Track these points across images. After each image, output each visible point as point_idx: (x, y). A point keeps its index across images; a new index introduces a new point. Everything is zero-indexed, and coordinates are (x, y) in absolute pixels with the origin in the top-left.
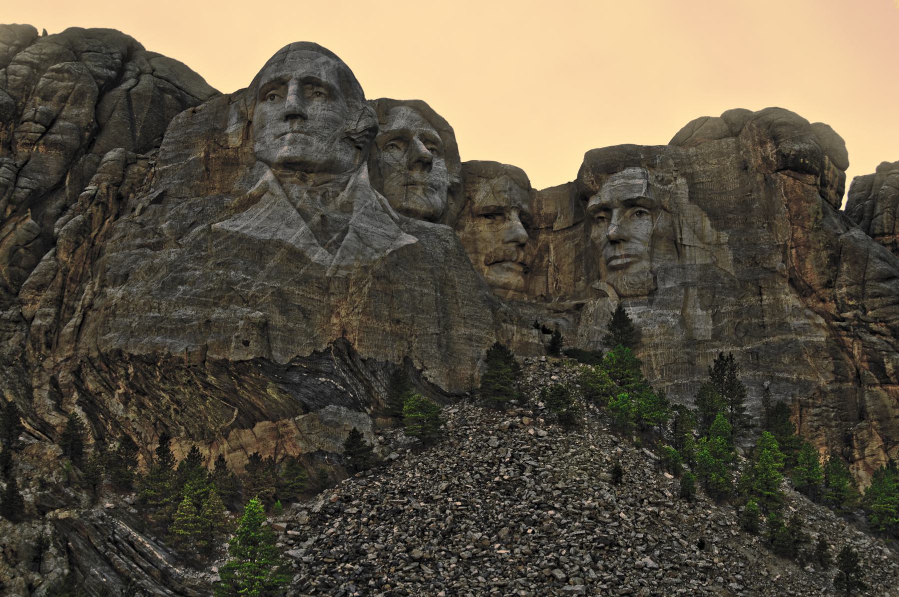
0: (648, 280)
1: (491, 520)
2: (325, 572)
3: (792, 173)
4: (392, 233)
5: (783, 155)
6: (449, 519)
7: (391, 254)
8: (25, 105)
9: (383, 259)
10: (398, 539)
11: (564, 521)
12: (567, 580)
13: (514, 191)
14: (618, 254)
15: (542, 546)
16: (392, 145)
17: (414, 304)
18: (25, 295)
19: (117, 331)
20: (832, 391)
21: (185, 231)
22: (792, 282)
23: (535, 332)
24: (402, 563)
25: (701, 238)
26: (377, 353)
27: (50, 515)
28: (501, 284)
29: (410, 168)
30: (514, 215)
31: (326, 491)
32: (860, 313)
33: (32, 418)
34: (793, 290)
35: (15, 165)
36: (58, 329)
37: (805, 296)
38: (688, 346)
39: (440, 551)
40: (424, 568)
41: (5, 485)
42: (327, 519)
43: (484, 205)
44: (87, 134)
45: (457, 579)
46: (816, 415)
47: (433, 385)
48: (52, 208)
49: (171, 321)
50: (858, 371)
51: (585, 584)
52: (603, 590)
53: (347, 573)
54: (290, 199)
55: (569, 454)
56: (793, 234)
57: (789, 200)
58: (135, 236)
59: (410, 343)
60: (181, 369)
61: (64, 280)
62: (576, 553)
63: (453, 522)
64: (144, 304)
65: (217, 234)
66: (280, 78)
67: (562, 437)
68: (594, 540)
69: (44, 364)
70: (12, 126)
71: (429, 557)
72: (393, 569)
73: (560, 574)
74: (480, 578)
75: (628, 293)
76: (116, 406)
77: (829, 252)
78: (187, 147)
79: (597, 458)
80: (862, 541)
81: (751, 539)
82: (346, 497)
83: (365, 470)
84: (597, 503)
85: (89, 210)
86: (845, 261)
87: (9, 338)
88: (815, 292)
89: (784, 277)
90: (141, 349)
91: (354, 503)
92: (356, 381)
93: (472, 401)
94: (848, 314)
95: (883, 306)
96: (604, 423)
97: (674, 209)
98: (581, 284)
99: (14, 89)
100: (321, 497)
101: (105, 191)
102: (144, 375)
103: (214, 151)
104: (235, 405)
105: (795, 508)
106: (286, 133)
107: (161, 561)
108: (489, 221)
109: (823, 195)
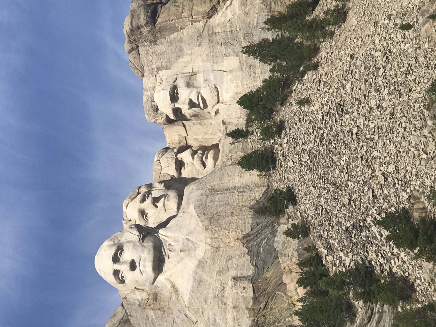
0: (211, 89)
1: (329, 165)
4: (189, 216)
5: (147, 23)
6: (330, 186)
9: (202, 221)
10: (339, 211)
12: (358, 126)
13: (168, 156)
15: (341, 139)
17: (223, 205)
22: (210, 18)
25: (189, 63)
28: (214, 162)
29: (156, 207)
30: (180, 156)
34: (213, 17)
38: (242, 69)
39: (345, 190)
45: (359, 182)
46: (275, 4)
47: (263, 195)
53: (357, 237)
56: (186, 18)
59: (243, 207)
60: (258, 320)
63: (330, 184)
65: (190, 303)
68: (338, 113)
71: (348, 196)
73: (355, 131)
78: (148, 319)
79: (298, 113)
81: (337, 35)
84: (320, 112)
89: (207, 21)
91: (322, 233)
93: (270, 175)
96: (281, 109)
97: (175, 77)
100: (319, 250)
103: (150, 305)
104: (275, 293)
108: (183, 168)
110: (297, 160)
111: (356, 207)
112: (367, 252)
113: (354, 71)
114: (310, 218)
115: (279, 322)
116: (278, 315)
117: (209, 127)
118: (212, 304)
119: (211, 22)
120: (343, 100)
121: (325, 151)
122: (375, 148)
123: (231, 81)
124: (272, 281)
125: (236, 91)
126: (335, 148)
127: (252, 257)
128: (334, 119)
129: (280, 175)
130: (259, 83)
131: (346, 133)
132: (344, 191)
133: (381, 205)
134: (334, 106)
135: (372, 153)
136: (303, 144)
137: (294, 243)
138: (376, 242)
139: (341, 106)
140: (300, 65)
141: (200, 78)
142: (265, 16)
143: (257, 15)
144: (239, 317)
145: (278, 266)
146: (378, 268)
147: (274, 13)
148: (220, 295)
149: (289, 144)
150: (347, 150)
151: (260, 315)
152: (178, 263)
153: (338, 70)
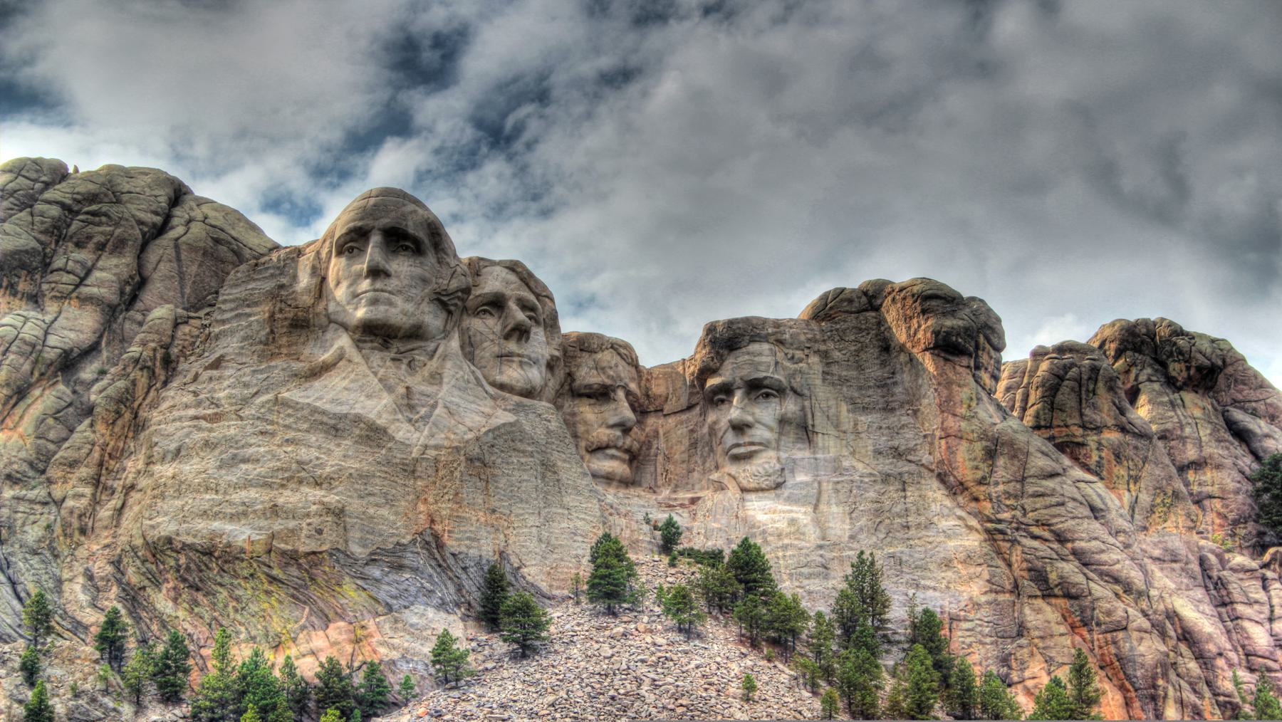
0: (774, 472)
4: (487, 410)
7: (486, 433)
8: (55, 251)
9: (477, 439)
13: (621, 368)
16: (485, 311)
18: (54, 472)
19: (166, 514)
21: (245, 401)
22: (942, 478)
23: (646, 528)
25: (837, 426)
26: (469, 547)
29: (507, 337)
30: (621, 394)
31: (410, 704)
32: (1018, 513)
34: (941, 486)
36: (93, 514)
38: (821, 547)
44: (128, 289)
48: (87, 372)
49: (230, 503)
50: (1016, 581)
54: (370, 368)
55: (692, 665)
57: (939, 384)
58: (187, 407)
60: (243, 560)
61: (102, 456)
65: (285, 404)
67: (684, 647)
69: (76, 553)
70: (37, 276)
75: (752, 486)
77: (984, 443)
78: (248, 306)
83: (457, 680)
87: (34, 522)
88: (967, 489)
89: (932, 471)
90: (195, 536)
92: (445, 578)
93: (578, 603)
94: (1006, 515)
95: (1046, 507)
97: (806, 392)
98: (696, 475)
99: (41, 232)
100: (406, 710)
101: (151, 354)
103: (281, 311)
104: (305, 603)
108: (592, 401)
109: (977, 380)
110: (616, 667)
115: (236, 611)
116: (253, 608)
117: (684, 466)
119: (929, 482)
123: (792, 522)
127: (392, 553)
129: (579, 624)
130: (787, 587)
140: (830, 683)
141: (801, 454)
147: (947, 626)
148: (303, 474)
151: (255, 565)
152: (380, 380)
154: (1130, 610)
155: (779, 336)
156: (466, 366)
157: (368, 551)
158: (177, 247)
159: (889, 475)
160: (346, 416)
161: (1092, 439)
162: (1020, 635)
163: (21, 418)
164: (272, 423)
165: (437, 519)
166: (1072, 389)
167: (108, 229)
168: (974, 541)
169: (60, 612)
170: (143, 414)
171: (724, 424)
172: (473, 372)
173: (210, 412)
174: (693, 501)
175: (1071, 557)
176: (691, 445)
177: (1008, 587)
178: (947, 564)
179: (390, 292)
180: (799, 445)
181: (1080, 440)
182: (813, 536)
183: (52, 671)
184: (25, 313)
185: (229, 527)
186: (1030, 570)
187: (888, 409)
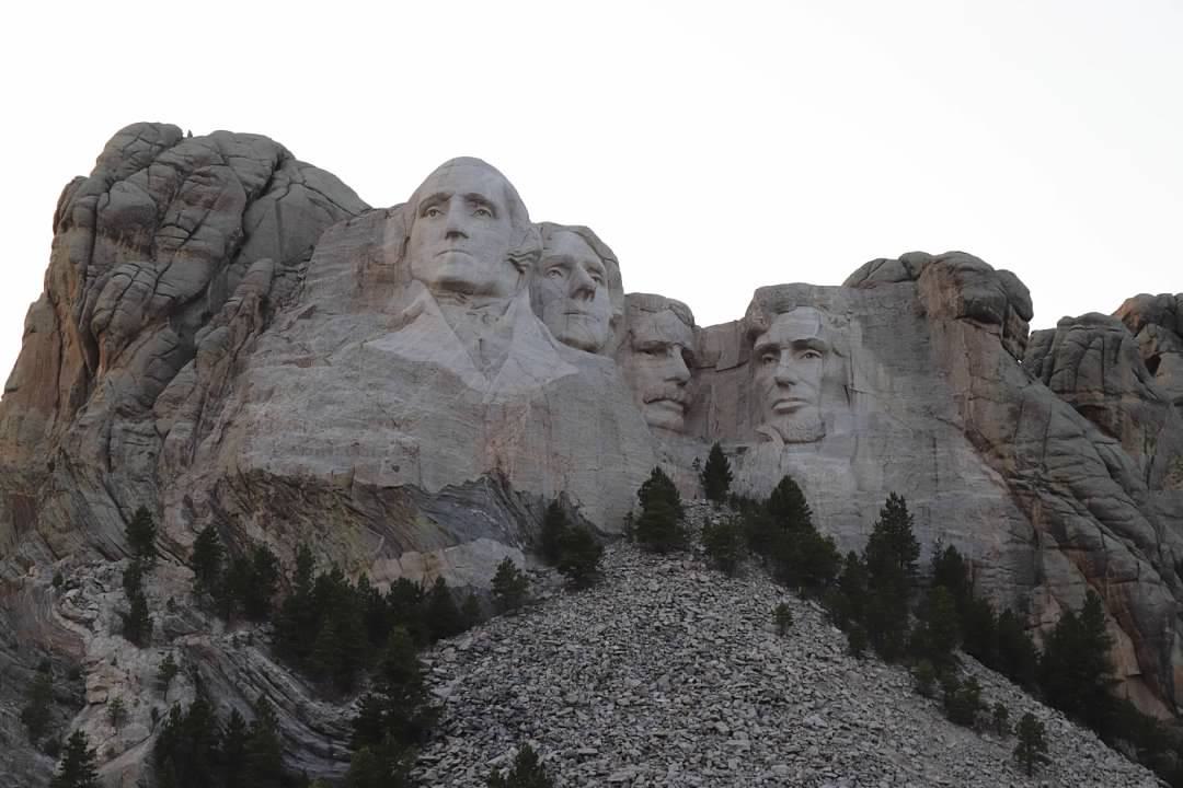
2: (473, 713)
3: (974, 322)
5: (966, 302)
6: (607, 662)
7: (550, 384)
8: (168, 208)
11: (728, 672)
12: (731, 734)
14: (786, 397)
15: (703, 697)
16: (554, 271)
18: (159, 408)
19: (258, 449)
20: (1010, 552)
21: (334, 349)
22: (969, 435)
24: (555, 709)
27: (178, 641)
29: (573, 296)
30: (677, 351)
31: (474, 628)
32: (1039, 470)
33: (162, 538)
34: (969, 443)
35: (155, 270)
36: (194, 447)
37: (981, 451)
38: (855, 496)
39: (596, 697)
40: (578, 712)
41: (130, 607)
42: (475, 657)
43: (645, 340)
44: (232, 243)
46: (989, 576)
47: (589, 523)
48: (193, 317)
49: (317, 441)
50: (1035, 532)
51: (750, 739)
52: (770, 747)
53: (496, 715)
54: (448, 322)
57: (970, 350)
58: (281, 352)
60: (326, 493)
61: (204, 394)
62: (740, 706)
63: (610, 667)
64: (289, 423)
65: (369, 352)
66: (442, 194)
67: (726, 584)
70: (151, 230)
71: (583, 702)
72: (545, 713)
73: (722, 727)
74: (638, 727)
76: (255, 531)
77: (1010, 405)
78: (340, 262)
80: (1042, 712)
81: (924, 703)
82: (496, 636)
84: (762, 656)
85: (232, 323)
86: (1026, 416)
87: (141, 452)
88: (993, 446)
89: (961, 429)
90: (284, 470)
92: (509, 514)
93: (629, 541)
95: (1066, 466)
96: (769, 572)
97: (848, 354)
99: (156, 190)
100: (469, 634)
101: (251, 302)
102: (285, 497)
103: (369, 267)
104: (381, 534)
105: (969, 672)
106: (446, 252)
107: (297, 695)
108: (649, 356)
110: (662, 600)
111: (559, 717)
112: (463, 735)
113: (846, 733)
114: (536, 618)
116: (334, 536)
118: (365, 399)
120: (788, 705)
121: (680, 661)
122: (684, 766)
124: (408, 528)
125: (809, 480)
126: (686, 682)
128: (748, 684)
129: (629, 561)
130: (823, 531)
131: (719, 706)
132: (592, 693)
133: (563, 771)
134: (774, 687)
135: (673, 758)
136: (696, 613)
137: (485, 578)
138: (483, 756)
139: (777, 702)
142: (966, 550)
143: (968, 535)
144: (335, 453)
145: (440, 544)
146: (427, 756)
148: (383, 415)
149: (696, 585)
150: (680, 706)
151: (337, 497)
153: (851, 699)
154: (1141, 563)
155: (823, 303)
156: (536, 322)
157: (441, 487)
158: (278, 209)
159: (920, 432)
160: (424, 364)
161: (1112, 404)
162: (1038, 583)
163: (132, 358)
164: (357, 369)
165: (504, 460)
166: (1095, 357)
167: (217, 189)
168: (998, 495)
169: (161, 534)
170: (239, 357)
171: (770, 381)
172: (541, 328)
173: (300, 357)
174: (741, 450)
175: (1087, 512)
176: (740, 399)
177: (1029, 538)
178: (972, 515)
179: (468, 253)
180: (841, 402)
181: (1102, 404)
182: (849, 485)
183: (153, 587)
184: (137, 263)
185: (314, 462)
186: (1048, 523)
187: (923, 372)
